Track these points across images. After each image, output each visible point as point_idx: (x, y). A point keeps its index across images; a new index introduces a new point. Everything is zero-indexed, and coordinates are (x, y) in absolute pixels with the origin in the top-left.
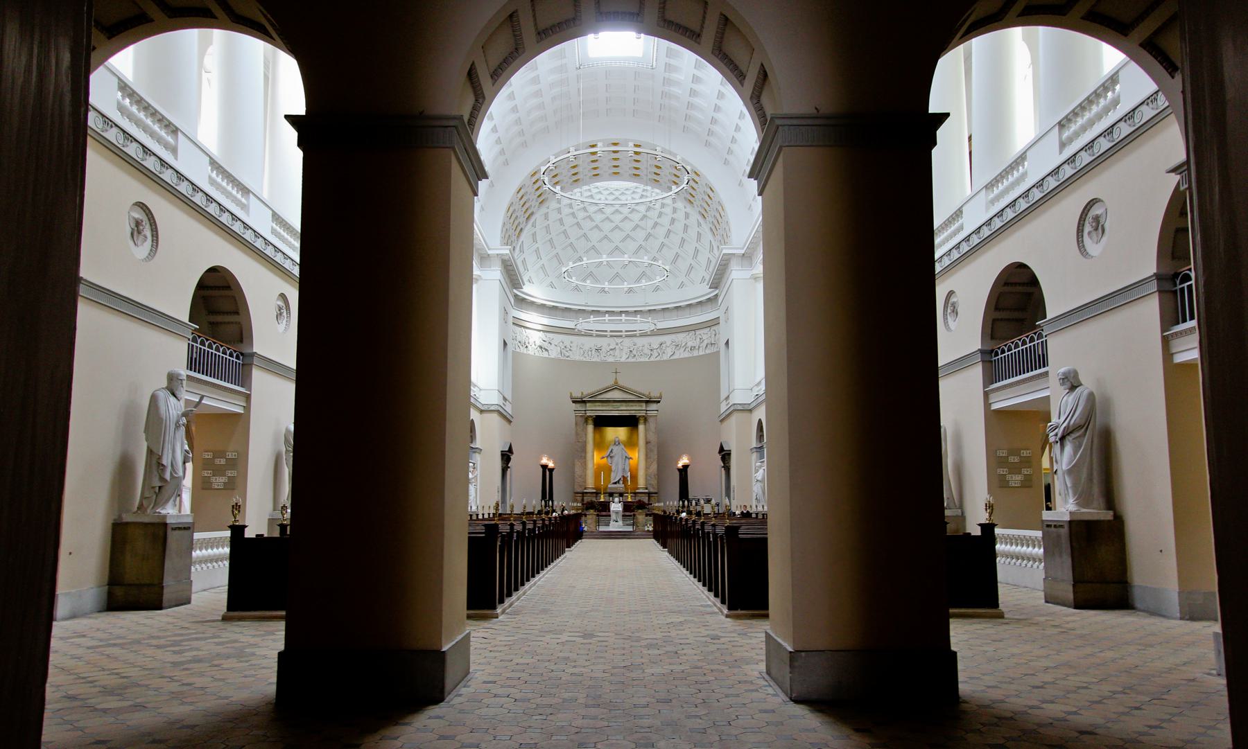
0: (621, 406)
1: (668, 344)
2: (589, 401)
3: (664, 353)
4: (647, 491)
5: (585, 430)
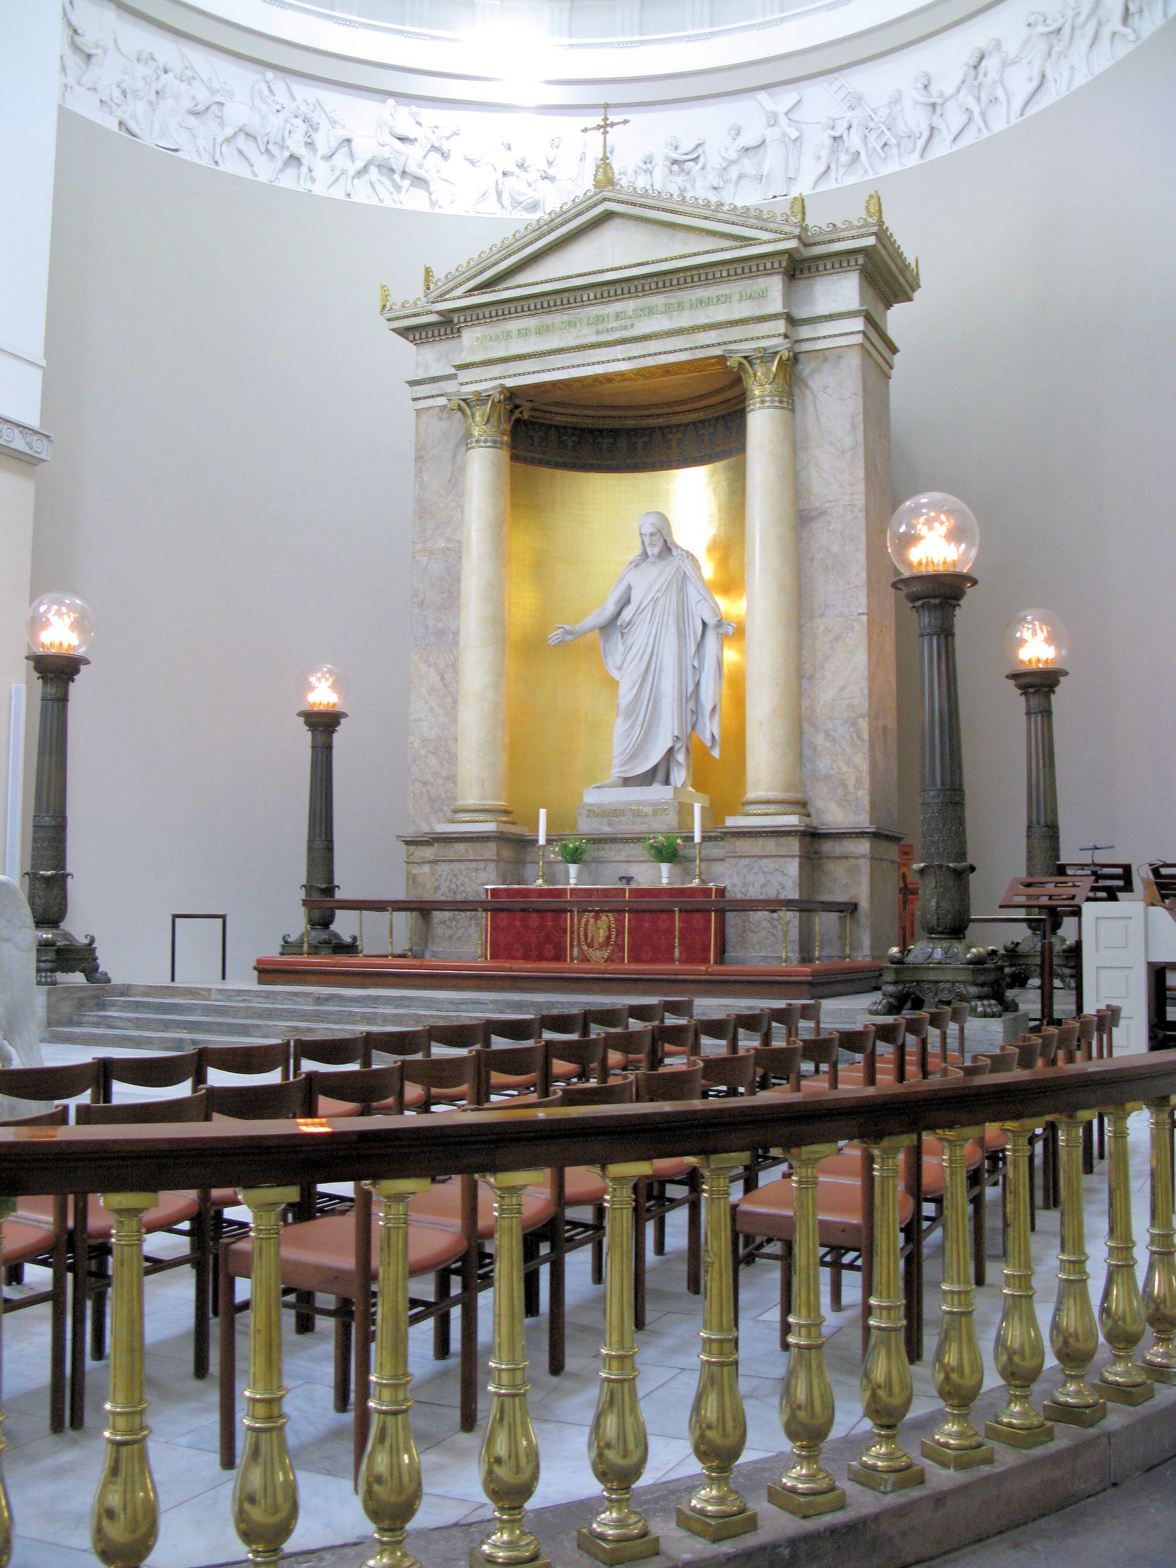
0: (650, 311)
1: (1011, 48)
2: (476, 314)
3: (994, 100)
4: (792, 820)
5: (455, 483)
